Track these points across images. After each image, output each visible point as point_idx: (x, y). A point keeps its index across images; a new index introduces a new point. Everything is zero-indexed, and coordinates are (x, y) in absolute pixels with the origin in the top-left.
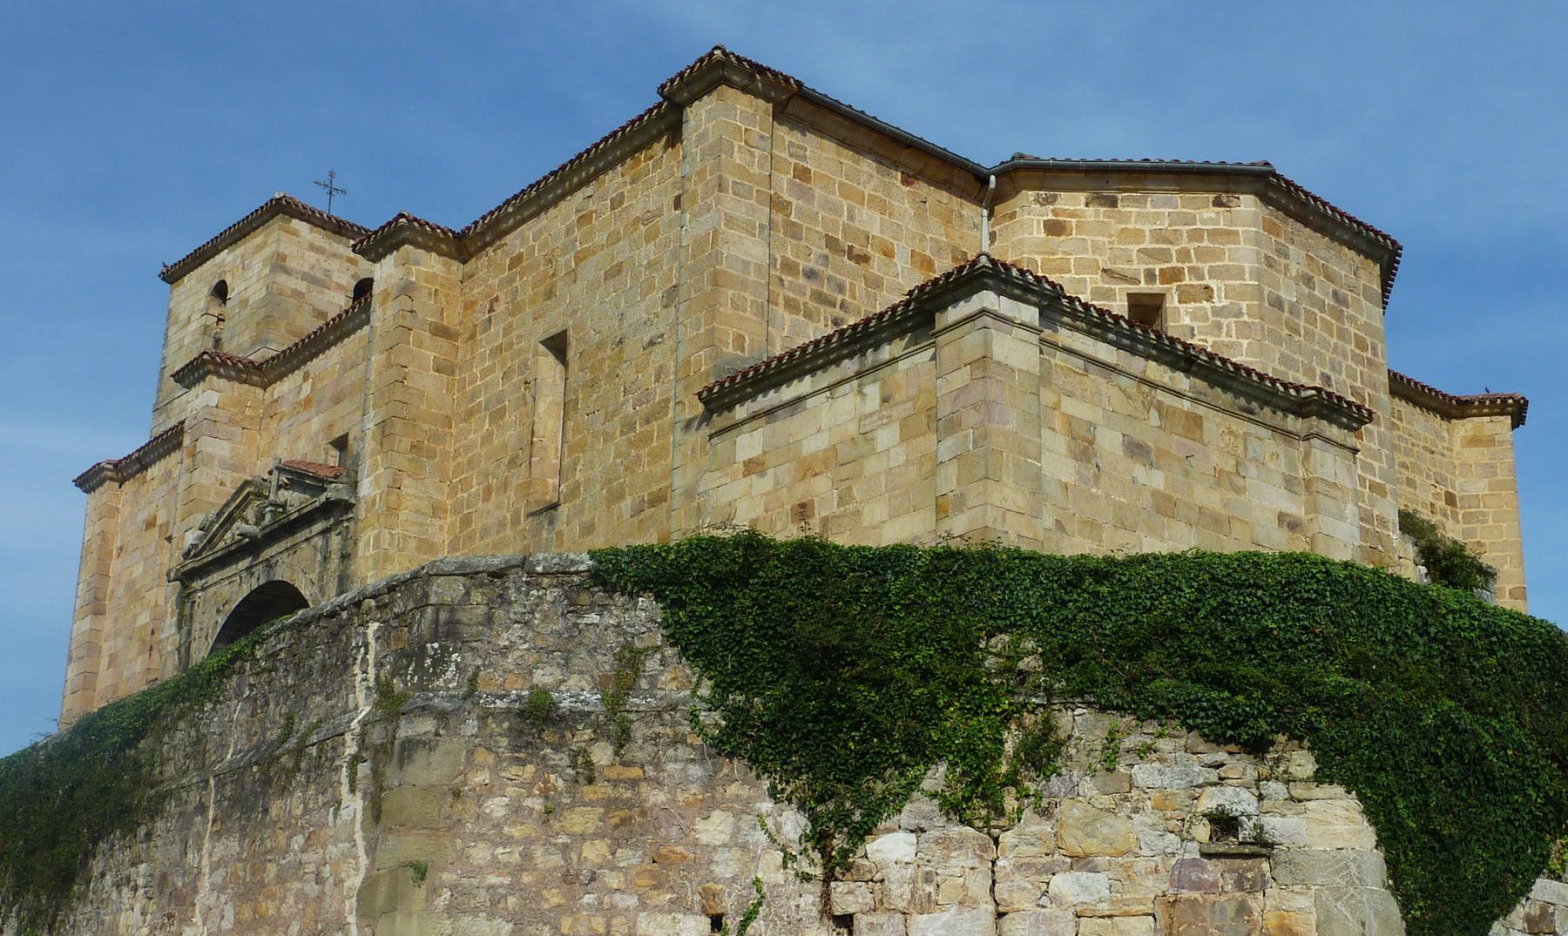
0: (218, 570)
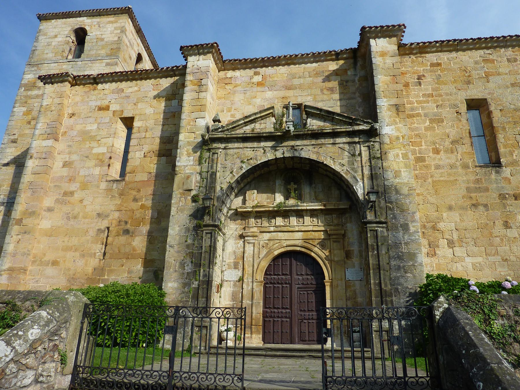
0: (238, 142)
